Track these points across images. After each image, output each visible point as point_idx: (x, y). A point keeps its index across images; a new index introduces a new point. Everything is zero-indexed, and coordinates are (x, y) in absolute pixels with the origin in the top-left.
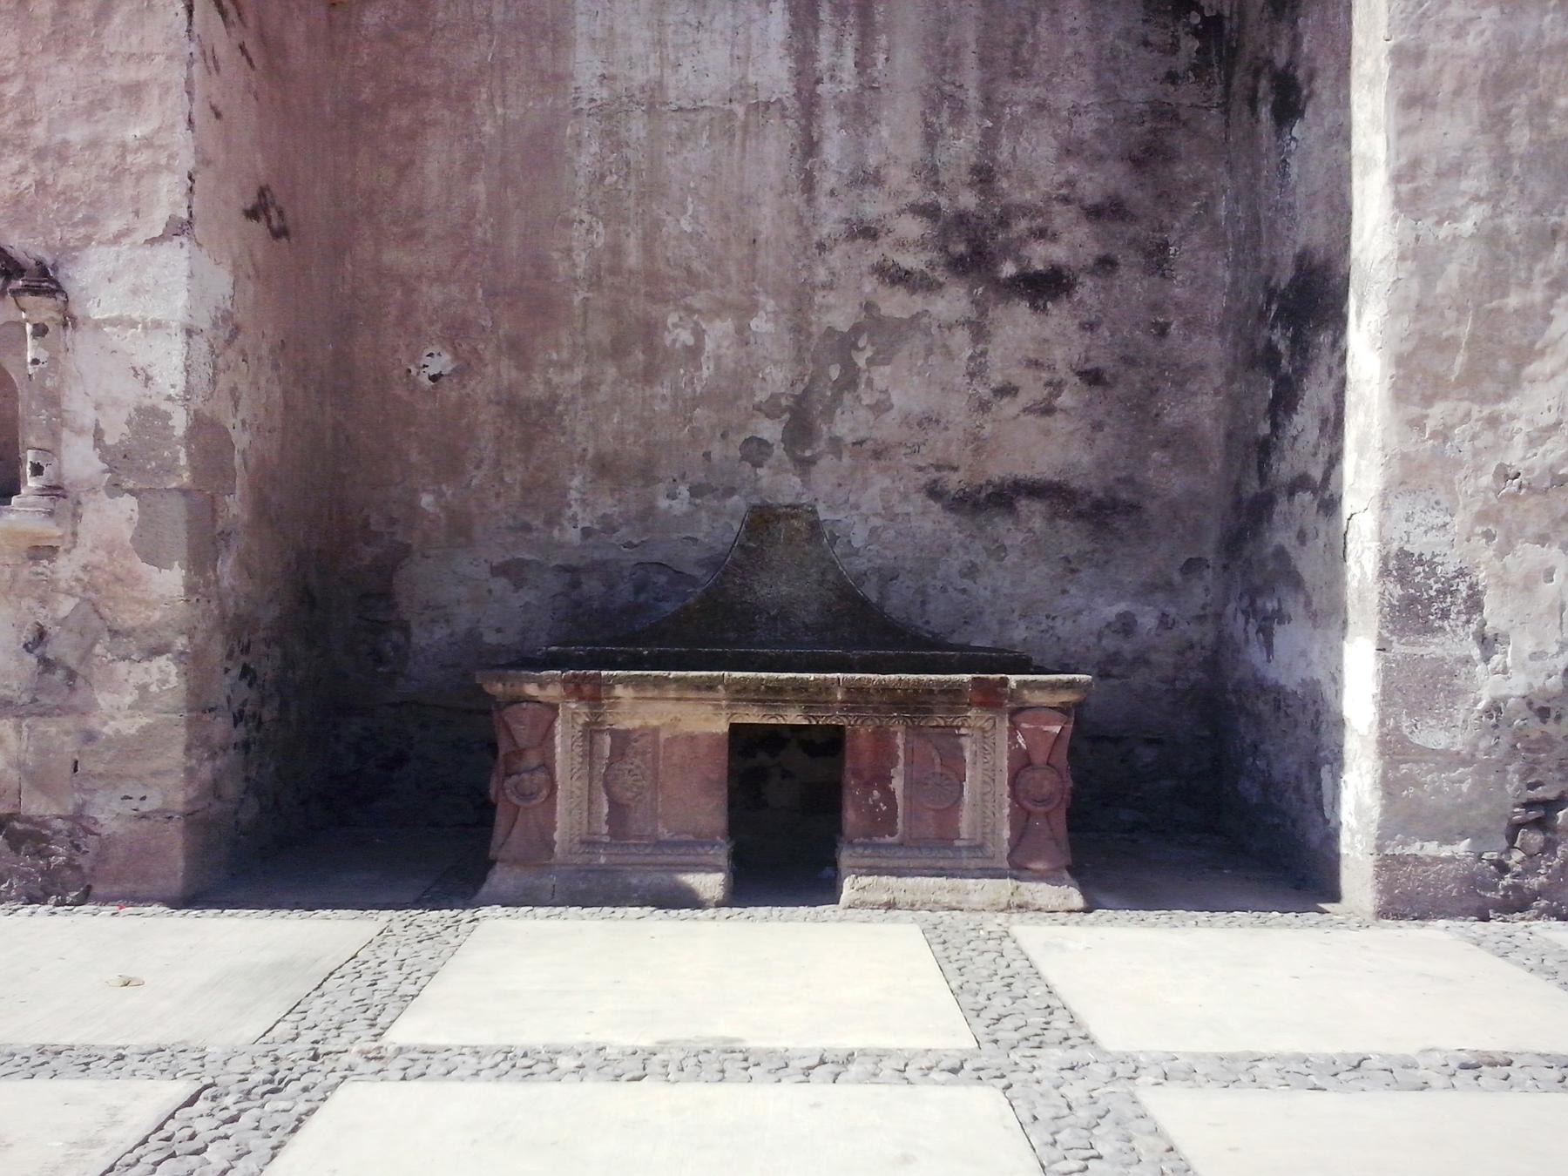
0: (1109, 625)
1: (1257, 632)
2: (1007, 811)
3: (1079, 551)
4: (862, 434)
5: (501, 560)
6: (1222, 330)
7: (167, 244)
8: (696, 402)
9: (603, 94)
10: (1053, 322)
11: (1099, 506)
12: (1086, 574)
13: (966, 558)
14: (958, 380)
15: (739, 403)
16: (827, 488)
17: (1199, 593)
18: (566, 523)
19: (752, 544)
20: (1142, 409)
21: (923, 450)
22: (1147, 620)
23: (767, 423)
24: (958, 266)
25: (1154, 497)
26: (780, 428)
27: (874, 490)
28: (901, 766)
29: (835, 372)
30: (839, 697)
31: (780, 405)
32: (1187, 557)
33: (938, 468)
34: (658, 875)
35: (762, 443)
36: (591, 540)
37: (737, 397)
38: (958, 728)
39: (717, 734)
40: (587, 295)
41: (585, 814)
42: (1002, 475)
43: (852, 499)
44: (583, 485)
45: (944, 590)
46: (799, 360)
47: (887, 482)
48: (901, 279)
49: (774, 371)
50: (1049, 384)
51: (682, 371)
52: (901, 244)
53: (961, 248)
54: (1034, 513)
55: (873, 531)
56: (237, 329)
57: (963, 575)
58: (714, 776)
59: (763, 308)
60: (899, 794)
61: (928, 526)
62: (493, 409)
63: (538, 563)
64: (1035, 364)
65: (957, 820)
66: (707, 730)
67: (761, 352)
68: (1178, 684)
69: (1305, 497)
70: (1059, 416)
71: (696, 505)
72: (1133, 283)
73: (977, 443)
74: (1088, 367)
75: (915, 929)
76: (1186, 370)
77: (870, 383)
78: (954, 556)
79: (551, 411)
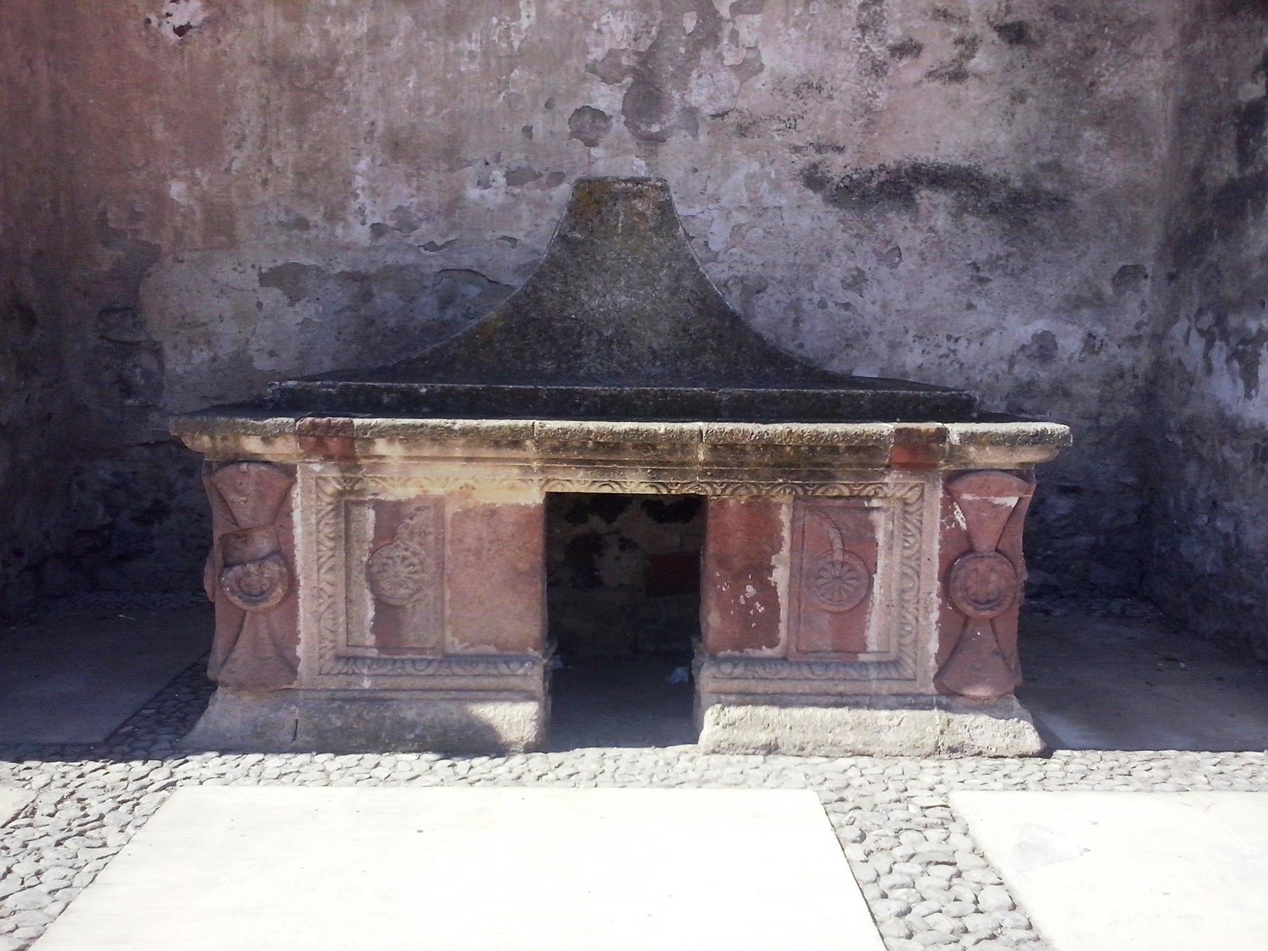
0: (1023, 347)
1: (1228, 360)
2: (935, 615)
3: (991, 256)
5: (271, 265)
8: (514, 59)
11: (1016, 198)
12: (997, 284)
13: (851, 264)
14: (846, 35)
15: (568, 62)
18: (351, 218)
19: (577, 235)
21: (801, 125)
22: (1070, 343)
23: (604, 88)
25: (1085, 188)
26: (620, 96)
27: (739, 176)
28: (785, 551)
29: (690, 23)
30: (701, 457)
31: (620, 65)
32: (1122, 264)
33: (819, 149)
34: (443, 705)
35: (598, 114)
36: (382, 241)
38: (869, 498)
39: (527, 507)
41: (342, 619)
42: (899, 158)
43: (710, 190)
44: (371, 168)
45: (822, 305)
47: (755, 167)
49: (612, 20)
51: (495, 20)
55: (737, 229)
57: (847, 286)
58: (523, 566)
61: (805, 223)
62: (257, 71)
63: (318, 269)
64: (944, 15)
65: (862, 625)
66: (514, 501)
68: (1104, 421)
70: (972, 82)
71: (513, 195)
73: (869, 116)
74: (1009, 20)
75: (811, 801)
76: (1131, 26)
77: (734, 35)
78: (836, 262)
79: (330, 71)
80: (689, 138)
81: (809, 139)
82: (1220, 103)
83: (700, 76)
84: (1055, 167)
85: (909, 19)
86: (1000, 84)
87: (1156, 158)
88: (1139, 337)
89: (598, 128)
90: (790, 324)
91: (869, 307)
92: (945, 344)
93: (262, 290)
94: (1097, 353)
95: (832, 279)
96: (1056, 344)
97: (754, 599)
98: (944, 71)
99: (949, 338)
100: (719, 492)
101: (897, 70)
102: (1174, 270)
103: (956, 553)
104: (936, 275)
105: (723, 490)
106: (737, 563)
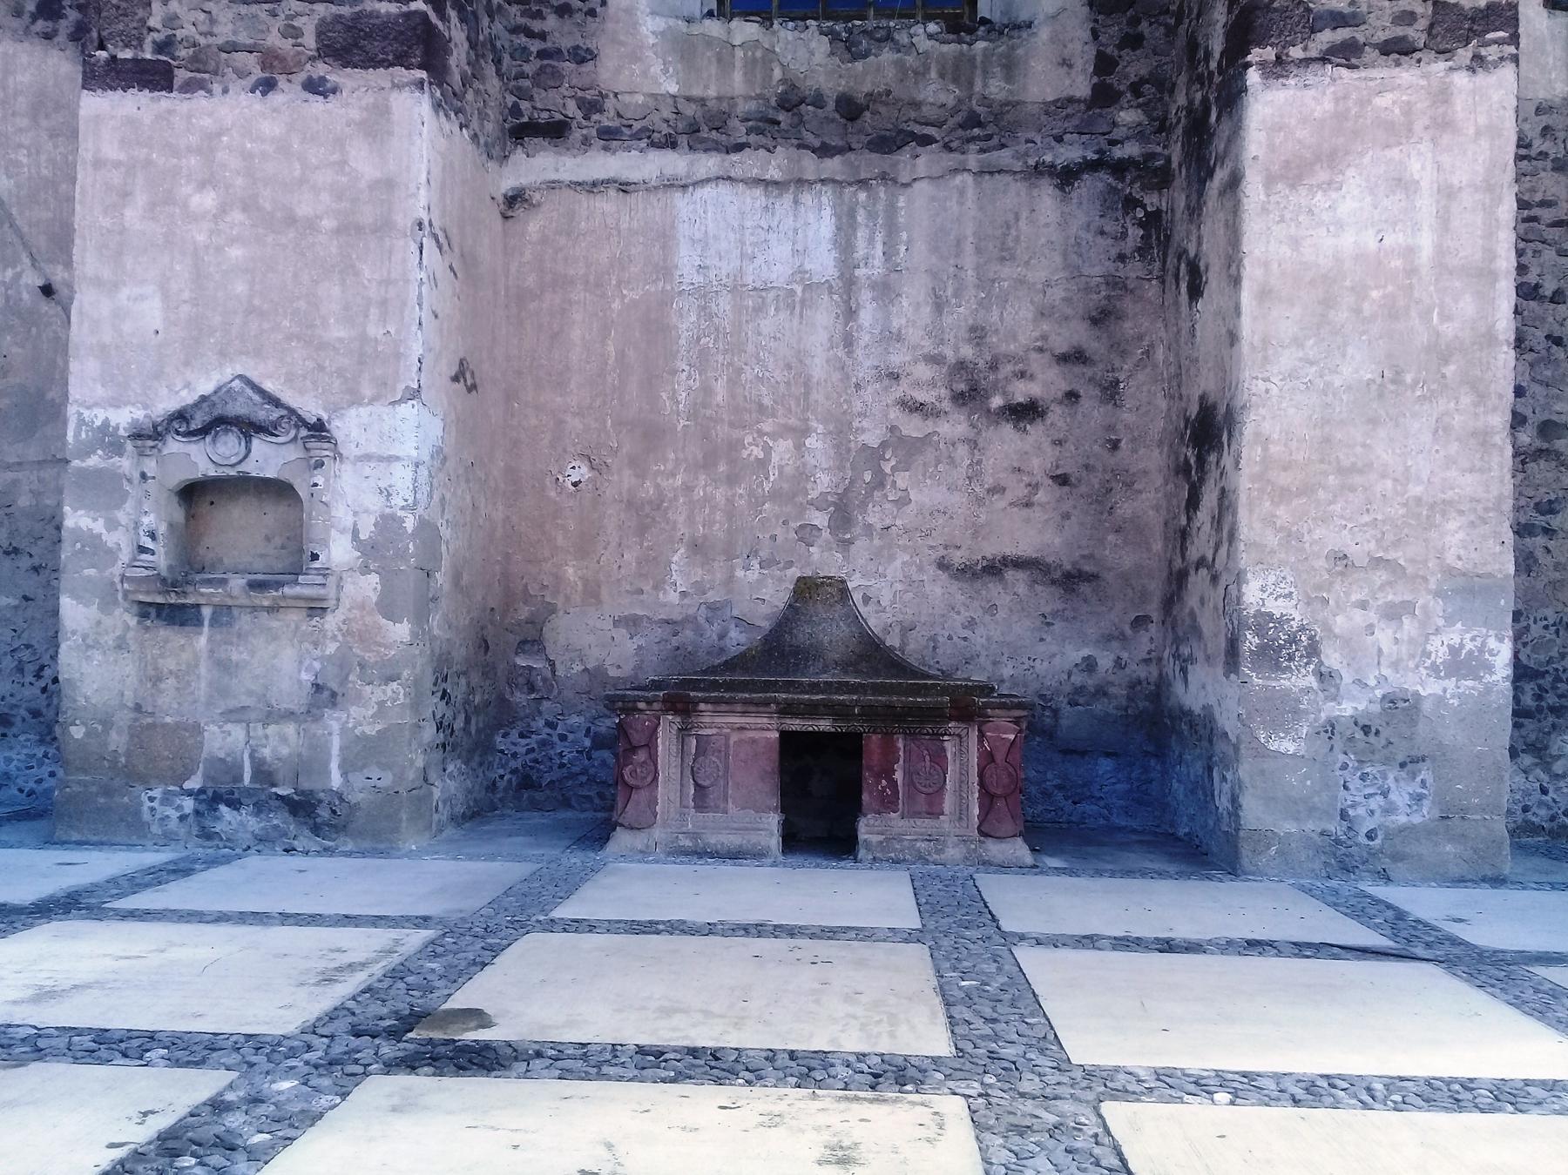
2: (977, 795)
4: (888, 522)
6: (1160, 443)
9: (698, 279)
10: (1030, 439)
12: (1058, 626)
13: (967, 614)
14: (960, 482)
16: (861, 562)
17: (1144, 642)
20: (1102, 499)
22: (1105, 662)
24: (959, 399)
25: (1110, 570)
27: (898, 563)
29: (868, 477)
37: (795, 495)
38: (943, 735)
45: (950, 638)
46: (841, 468)
47: (907, 558)
48: (917, 409)
53: (962, 387)
54: (1017, 580)
56: (445, 459)
59: (815, 431)
65: (941, 803)
67: (813, 462)
69: (1203, 572)
70: (1036, 508)
72: (1093, 410)
74: (1059, 472)
75: (904, 876)
76: (1134, 474)
79: (659, 507)
84: (1091, 557)
91: (979, 639)
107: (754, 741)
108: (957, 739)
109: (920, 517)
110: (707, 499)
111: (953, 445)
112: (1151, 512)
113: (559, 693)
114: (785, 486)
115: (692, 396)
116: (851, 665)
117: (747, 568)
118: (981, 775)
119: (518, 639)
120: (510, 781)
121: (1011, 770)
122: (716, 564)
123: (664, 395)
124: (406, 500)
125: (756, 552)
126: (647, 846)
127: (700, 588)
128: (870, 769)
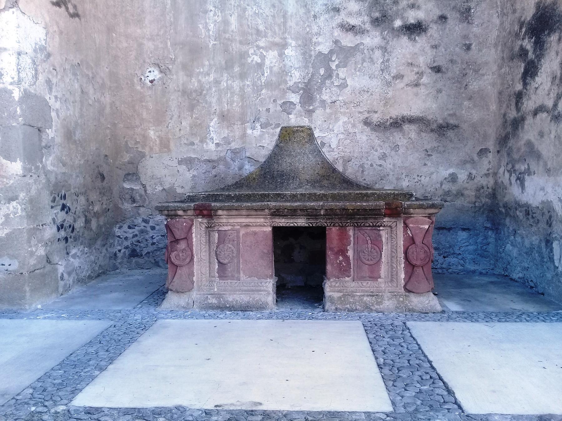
1: (516, 180)
2: (403, 265)
3: (431, 147)
4: (334, 98)
6: (496, 45)
7: (6, 12)
10: (418, 45)
11: (441, 127)
15: (281, 87)
16: (319, 123)
17: (486, 164)
18: (208, 141)
21: (362, 104)
22: (462, 176)
23: (293, 95)
24: (376, 22)
27: (340, 123)
29: (322, 71)
30: (322, 213)
31: (298, 87)
32: (481, 148)
37: (279, 85)
38: (379, 226)
40: (214, 42)
43: (331, 127)
45: (371, 165)
46: (306, 67)
47: (346, 119)
48: (350, 29)
49: (295, 72)
50: (418, 73)
52: (350, 14)
53: (377, 15)
54: (411, 130)
56: (49, 55)
57: (380, 159)
58: (265, 251)
59: (290, 45)
60: (351, 258)
65: (379, 269)
67: (290, 64)
68: (477, 204)
74: (435, 65)
75: (359, 324)
77: (338, 74)
80: (323, 110)
81: (365, 109)
82: (511, 91)
83: (326, 89)
85: (399, 67)
86: (432, 87)
87: (491, 110)
88: (489, 174)
89: (291, 108)
90: (360, 172)
91: (388, 165)
92: (416, 178)
93: (179, 166)
94: (473, 180)
95: (375, 157)
96: (457, 177)
97: (342, 261)
98: (412, 84)
99: (418, 176)
100: (329, 225)
101: (395, 84)
102: (499, 150)
103: (409, 244)
104: (412, 154)
105: (331, 224)
106: (336, 250)
107: (255, 233)
108: (389, 229)
109: (353, 95)
110: (229, 88)
111: (372, 50)
112: (489, 87)
113: (150, 203)
114: (274, 79)
115: (217, 26)
116: (317, 182)
117: (253, 128)
118: (406, 253)
119: (125, 173)
120: (124, 253)
121: (426, 249)
122: (235, 127)
123: (201, 26)
124: (13, 78)
125: (259, 119)
126: (188, 304)
127: (227, 141)
128: (331, 249)
